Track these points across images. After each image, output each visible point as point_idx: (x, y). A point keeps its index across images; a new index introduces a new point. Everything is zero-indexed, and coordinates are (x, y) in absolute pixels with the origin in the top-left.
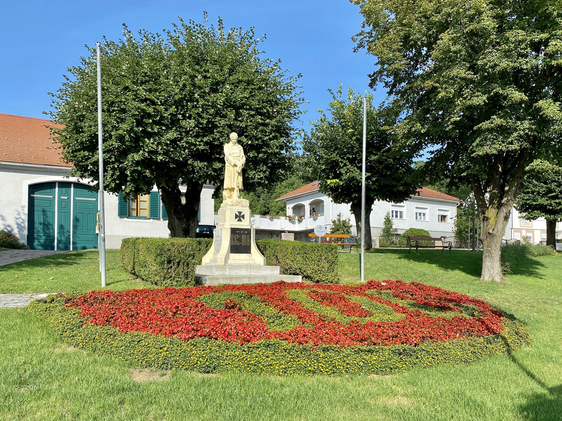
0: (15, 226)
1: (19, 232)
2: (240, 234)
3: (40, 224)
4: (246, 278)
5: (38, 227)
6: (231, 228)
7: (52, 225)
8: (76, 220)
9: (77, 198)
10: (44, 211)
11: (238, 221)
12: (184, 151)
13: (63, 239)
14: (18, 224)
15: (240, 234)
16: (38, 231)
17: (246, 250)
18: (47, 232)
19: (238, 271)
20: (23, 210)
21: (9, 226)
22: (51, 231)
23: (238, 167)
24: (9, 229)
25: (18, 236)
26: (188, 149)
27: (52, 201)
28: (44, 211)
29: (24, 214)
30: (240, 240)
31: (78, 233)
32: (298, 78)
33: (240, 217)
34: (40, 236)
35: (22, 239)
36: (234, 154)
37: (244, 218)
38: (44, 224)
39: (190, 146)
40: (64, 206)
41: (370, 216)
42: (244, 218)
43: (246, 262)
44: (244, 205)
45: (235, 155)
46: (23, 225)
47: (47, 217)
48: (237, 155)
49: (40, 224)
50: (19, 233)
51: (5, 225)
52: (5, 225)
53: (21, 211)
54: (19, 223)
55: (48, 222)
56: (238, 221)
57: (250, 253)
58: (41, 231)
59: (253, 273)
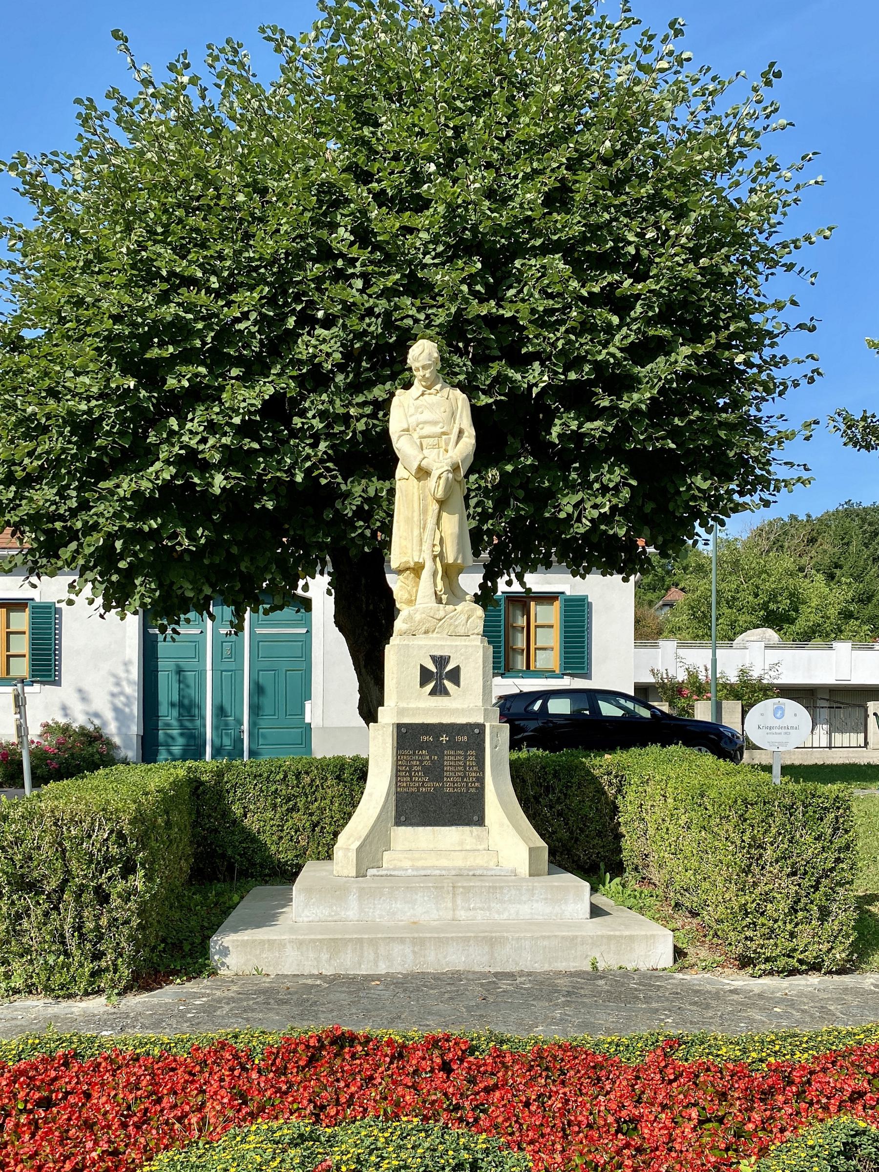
0: (109, 715)
1: (119, 729)
2: (436, 748)
3: (173, 705)
4: (402, 940)
5: (168, 715)
6: (399, 726)
7: (199, 708)
8: (258, 690)
9: (259, 631)
10: (179, 671)
11: (433, 693)
12: (314, 446)
13: (227, 741)
14: (116, 709)
15: (436, 748)
16: (168, 725)
17: (466, 810)
18: (188, 724)
19: (398, 905)
20: (127, 671)
21: (97, 715)
22: (198, 722)
23: (435, 474)
24: (97, 722)
25: (117, 740)
26: (329, 436)
27: (197, 644)
28: (179, 671)
29: (129, 682)
30: (435, 772)
31: (263, 724)
32: (764, 91)
33: (440, 677)
34: (173, 738)
35: (127, 747)
36: (430, 424)
37: (457, 682)
38: (181, 705)
39: (329, 426)
40: (227, 656)
41: (357, 685)
42: (457, 682)
43: (459, 861)
44: (461, 630)
45: (428, 430)
46: (127, 710)
47: (188, 686)
48: (437, 429)
49: (173, 705)
50: (120, 733)
51: (87, 713)
52: (87, 713)
53: (123, 675)
54: (120, 705)
55: (191, 701)
56: (433, 693)
57: (481, 822)
58: (174, 723)
59: (472, 913)
